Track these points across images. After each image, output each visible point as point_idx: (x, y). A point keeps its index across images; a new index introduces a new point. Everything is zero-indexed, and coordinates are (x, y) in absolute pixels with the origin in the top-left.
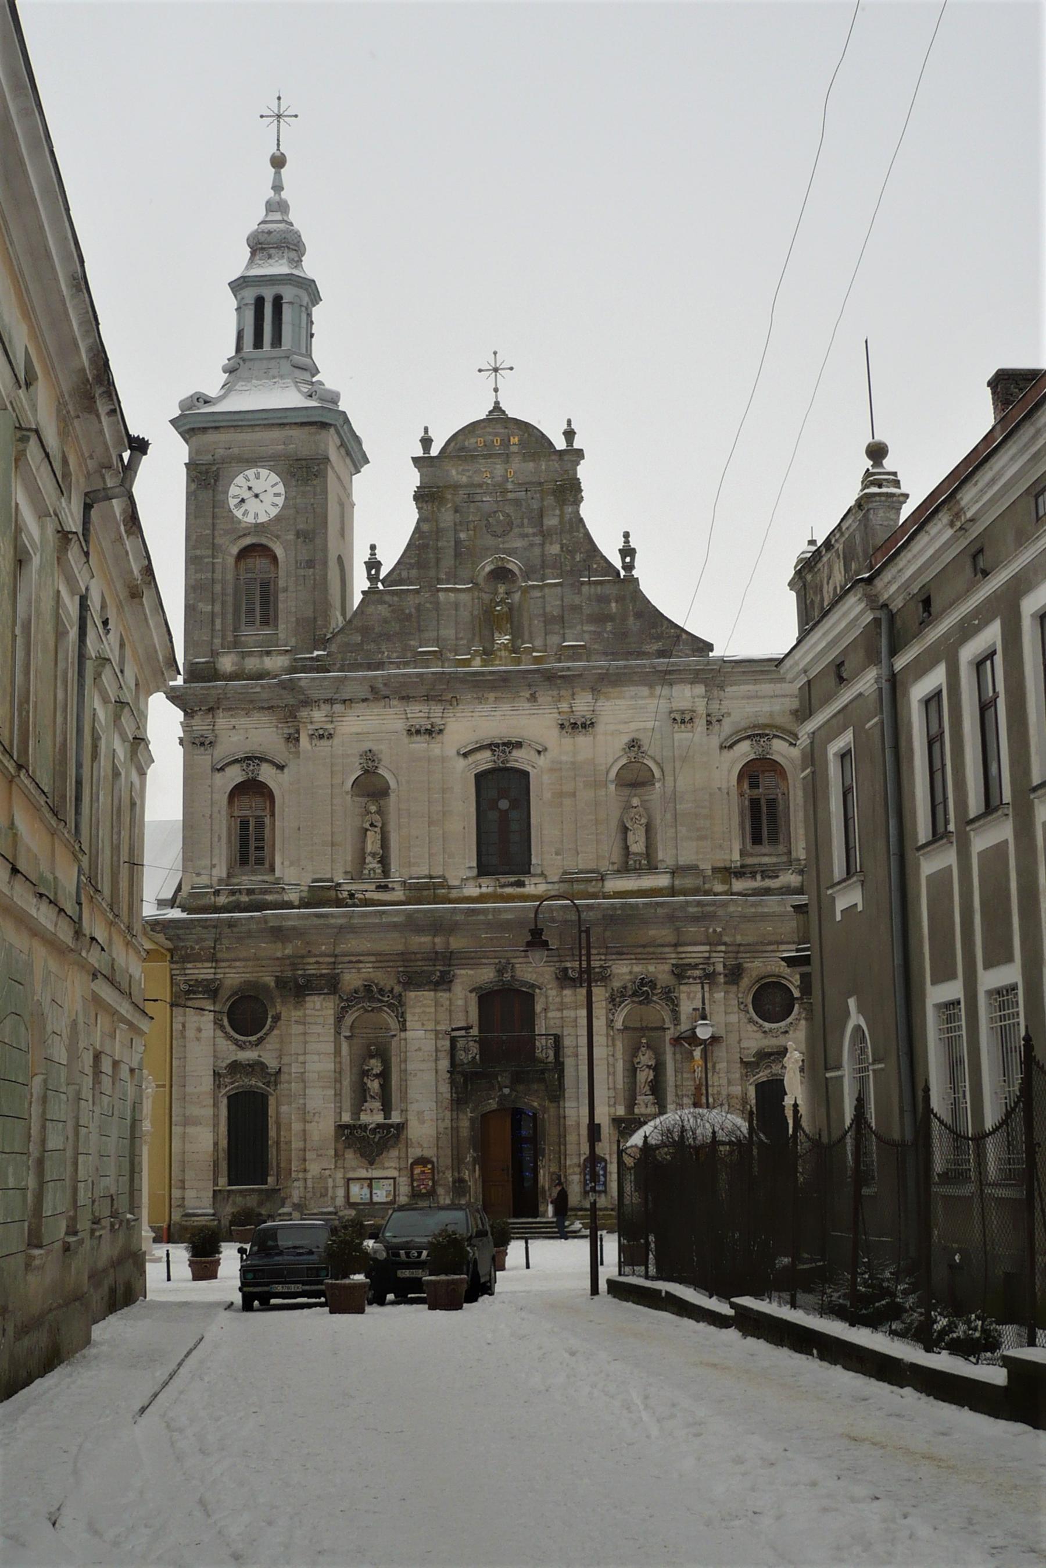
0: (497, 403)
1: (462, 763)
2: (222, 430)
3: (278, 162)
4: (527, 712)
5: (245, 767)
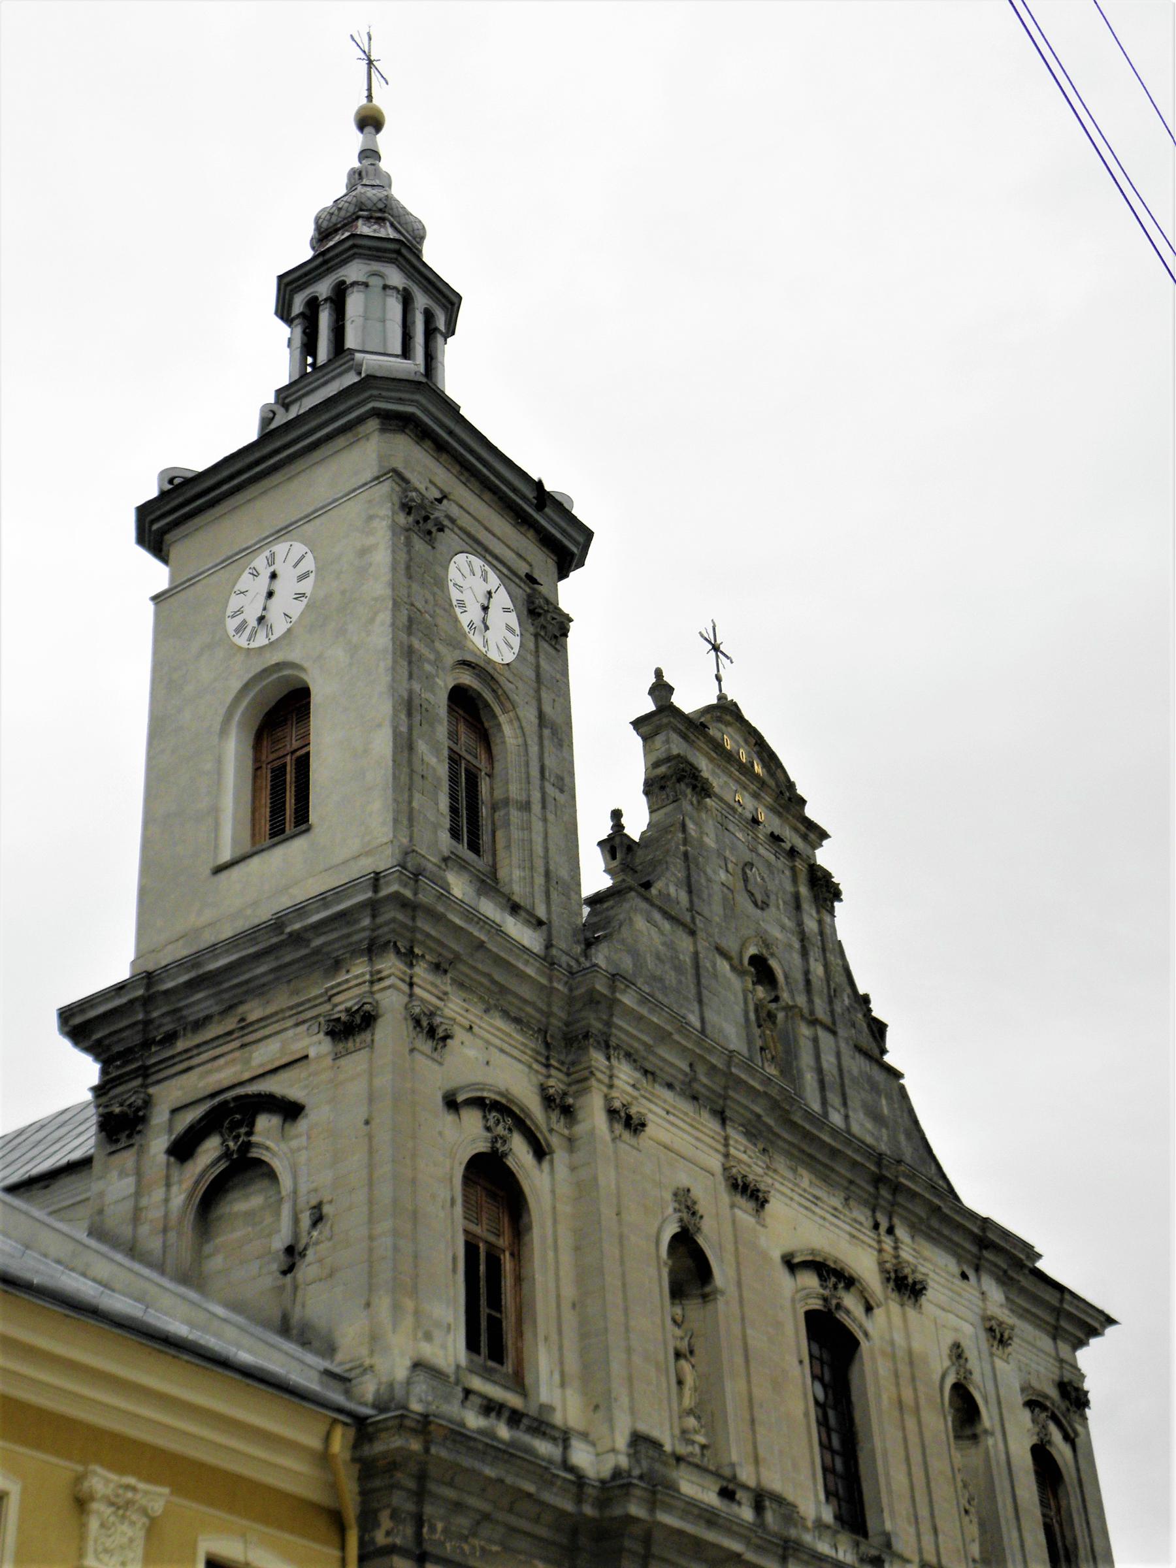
0: (722, 697)
1: (786, 1283)
2: (444, 456)
3: (370, 121)
4: (848, 1228)
5: (491, 1123)
